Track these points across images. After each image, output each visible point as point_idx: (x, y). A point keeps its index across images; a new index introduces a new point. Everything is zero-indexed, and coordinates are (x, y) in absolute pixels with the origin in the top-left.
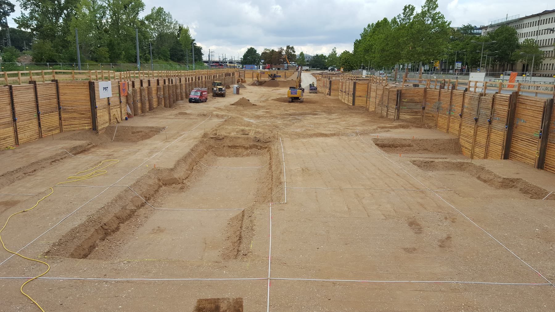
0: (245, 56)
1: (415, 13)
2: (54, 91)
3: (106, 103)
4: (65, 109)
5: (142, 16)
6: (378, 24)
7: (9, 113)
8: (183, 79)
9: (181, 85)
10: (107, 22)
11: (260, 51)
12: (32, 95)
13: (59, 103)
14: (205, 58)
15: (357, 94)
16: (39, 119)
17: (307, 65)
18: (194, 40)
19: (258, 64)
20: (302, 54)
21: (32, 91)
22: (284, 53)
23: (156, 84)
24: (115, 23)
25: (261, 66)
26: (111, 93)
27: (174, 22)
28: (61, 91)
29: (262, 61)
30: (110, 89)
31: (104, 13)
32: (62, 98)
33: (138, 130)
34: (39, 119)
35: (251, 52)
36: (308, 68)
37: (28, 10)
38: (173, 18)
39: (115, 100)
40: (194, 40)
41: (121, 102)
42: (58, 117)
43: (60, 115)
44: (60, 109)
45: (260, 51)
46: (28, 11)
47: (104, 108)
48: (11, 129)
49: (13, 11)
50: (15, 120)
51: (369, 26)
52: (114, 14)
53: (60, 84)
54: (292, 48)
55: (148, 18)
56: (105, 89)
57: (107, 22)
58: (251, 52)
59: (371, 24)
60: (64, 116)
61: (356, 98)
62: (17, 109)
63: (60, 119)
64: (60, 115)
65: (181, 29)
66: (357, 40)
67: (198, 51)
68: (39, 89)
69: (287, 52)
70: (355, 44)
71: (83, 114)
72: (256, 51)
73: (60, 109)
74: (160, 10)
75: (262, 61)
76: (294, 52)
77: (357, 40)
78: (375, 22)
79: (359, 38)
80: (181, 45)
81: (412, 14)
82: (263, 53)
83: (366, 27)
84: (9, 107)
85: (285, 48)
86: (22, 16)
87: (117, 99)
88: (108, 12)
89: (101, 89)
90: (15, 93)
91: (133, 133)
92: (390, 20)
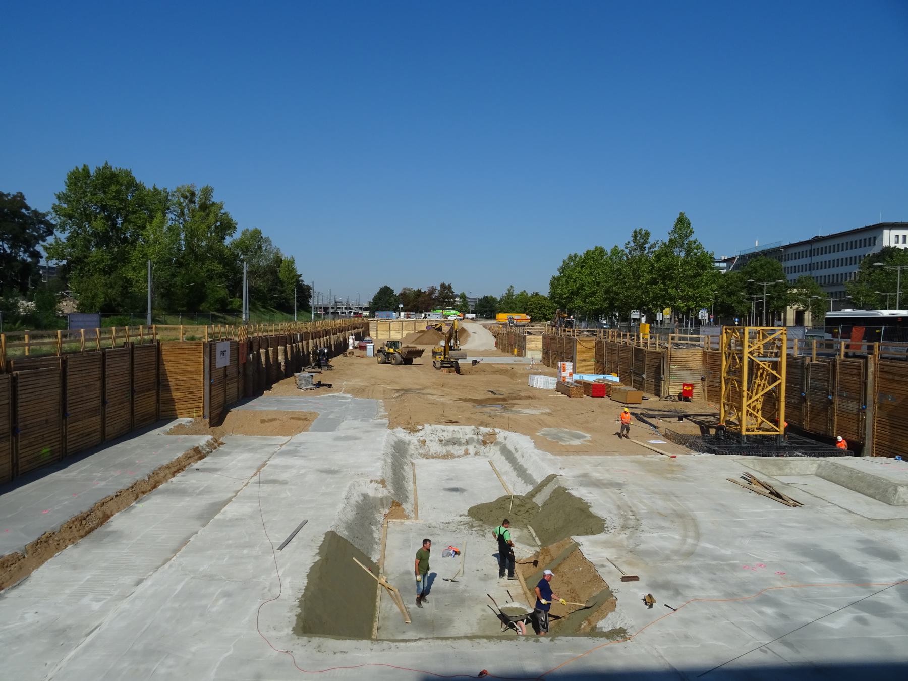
1: (651, 240)
3: (221, 374)
5: (228, 241)
11: (397, 292)
12: (127, 364)
16: (132, 403)
17: (473, 312)
18: (300, 276)
19: (396, 310)
20: (463, 296)
22: (437, 294)
25: (402, 314)
29: (401, 306)
30: (228, 353)
33: (270, 417)
34: (132, 403)
35: (385, 292)
36: (474, 316)
37: (67, 232)
38: (274, 244)
39: (232, 371)
40: (300, 276)
41: (239, 373)
42: (155, 398)
43: (158, 395)
44: (159, 383)
46: (67, 234)
47: (220, 383)
48: (98, 418)
49: (51, 233)
50: (104, 402)
51: (570, 257)
54: (450, 286)
56: (223, 352)
58: (385, 292)
59: (572, 255)
62: (108, 387)
63: (158, 401)
64: (158, 395)
65: (279, 261)
66: (554, 278)
67: (304, 292)
68: (137, 353)
70: (552, 284)
72: (392, 291)
73: (159, 383)
75: (401, 306)
77: (554, 278)
78: (581, 253)
79: (557, 274)
80: (282, 283)
81: (646, 242)
83: (566, 258)
84: (99, 384)
85: (439, 288)
87: (235, 370)
88: (182, 236)
90: (108, 361)
91: (263, 421)
92: (608, 250)
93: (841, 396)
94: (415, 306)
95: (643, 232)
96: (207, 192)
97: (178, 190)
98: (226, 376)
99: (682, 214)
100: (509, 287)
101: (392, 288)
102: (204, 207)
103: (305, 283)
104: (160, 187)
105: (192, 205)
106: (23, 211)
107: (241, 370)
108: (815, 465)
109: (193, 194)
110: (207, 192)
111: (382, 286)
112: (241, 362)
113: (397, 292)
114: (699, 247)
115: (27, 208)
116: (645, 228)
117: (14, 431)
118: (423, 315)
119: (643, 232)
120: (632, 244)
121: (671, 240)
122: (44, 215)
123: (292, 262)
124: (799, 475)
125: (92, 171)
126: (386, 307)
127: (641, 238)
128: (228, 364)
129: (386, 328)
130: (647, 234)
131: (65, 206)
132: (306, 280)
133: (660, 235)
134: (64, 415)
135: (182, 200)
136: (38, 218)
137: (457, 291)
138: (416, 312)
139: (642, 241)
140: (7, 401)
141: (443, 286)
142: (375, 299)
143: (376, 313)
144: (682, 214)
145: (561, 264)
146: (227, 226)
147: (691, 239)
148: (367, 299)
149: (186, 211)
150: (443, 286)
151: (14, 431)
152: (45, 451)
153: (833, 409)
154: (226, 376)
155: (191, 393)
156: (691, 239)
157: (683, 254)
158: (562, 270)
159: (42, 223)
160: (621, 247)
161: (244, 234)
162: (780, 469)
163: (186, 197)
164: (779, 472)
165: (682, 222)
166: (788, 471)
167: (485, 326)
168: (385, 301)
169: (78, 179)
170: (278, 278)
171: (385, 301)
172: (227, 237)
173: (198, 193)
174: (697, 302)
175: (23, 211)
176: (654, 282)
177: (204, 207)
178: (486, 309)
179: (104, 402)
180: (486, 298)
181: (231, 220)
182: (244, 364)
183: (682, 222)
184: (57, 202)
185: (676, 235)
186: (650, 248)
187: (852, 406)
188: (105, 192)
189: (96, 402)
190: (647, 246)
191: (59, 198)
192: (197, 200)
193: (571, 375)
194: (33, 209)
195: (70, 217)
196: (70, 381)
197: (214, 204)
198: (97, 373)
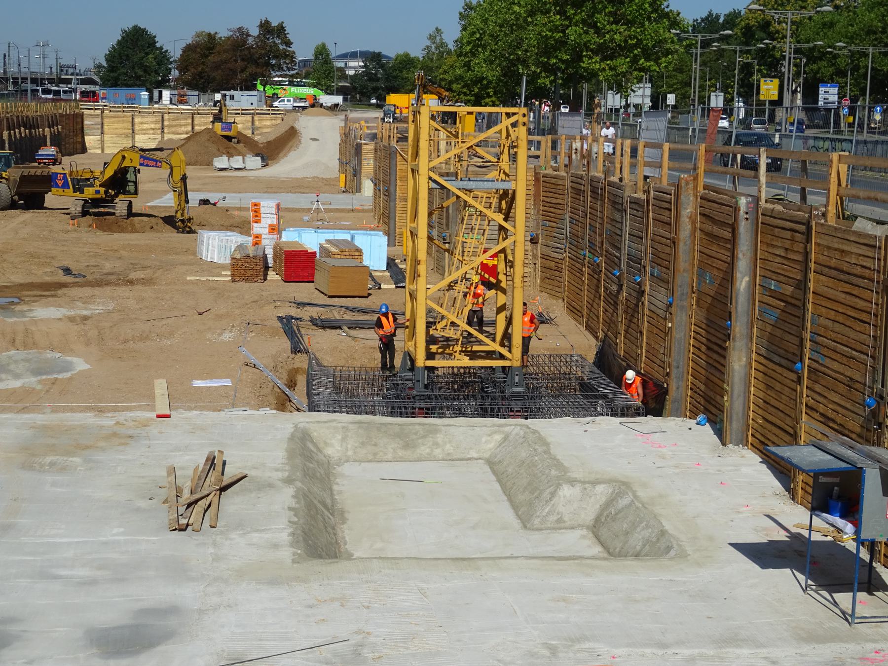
11: (173, 40)
17: (340, 91)
25: (166, 93)
36: (339, 99)
54: (280, 30)
76: (288, 43)
85: (255, 31)
93: (652, 275)
94: (200, 75)
101: (152, 30)
108: (498, 437)
111: (128, 25)
113: (173, 40)
118: (218, 96)
124: (449, 459)
126: (138, 78)
129: (123, 126)
138: (203, 90)
141: (265, 26)
142: (110, 58)
150: (265, 26)
153: (643, 303)
162: (407, 446)
164: (401, 453)
166: (424, 450)
168: (134, 63)
171: (134, 63)
174: (635, 60)
178: (376, 81)
187: (662, 297)
193: (272, 229)
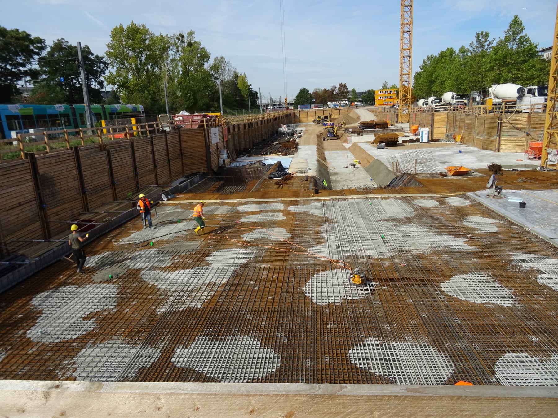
0: (298, 97)
1: (490, 39)
2: (177, 139)
3: (215, 148)
4: (186, 156)
5: (206, 66)
6: (442, 55)
7: (150, 161)
8: (259, 123)
9: (258, 128)
10: (178, 74)
11: (311, 91)
12: (164, 144)
13: (181, 150)
14: (259, 102)
15: (436, 125)
16: (169, 166)
17: (361, 102)
18: (250, 85)
20: (354, 91)
21: (164, 139)
23: (243, 128)
24: (186, 73)
26: (218, 138)
27: (234, 70)
28: (182, 138)
30: (217, 134)
31: (177, 65)
32: (183, 145)
34: (169, 166)
35: (304, 92)
37: (115, 68)
39: (221, 145)
40: (250, 85)
43: (182, 161)
44: (182, 155)
45: (389, 85)
49: (107, 68)
50: (155, 167)
51: (428, 58)
52: (185, 65)
53: (182, 133)
54: (345, 86)
55: (215, 68)
56: (215, 134)
57: (178, 74)
58: (304, 92)
59: (430, 56)
60: (185, 162)
61: (435, 130)
62: (156, 157)
63: (182, 164)
64: (182, 161)
65: (236, 76)
67: (254, 96)
69: (340, 89)
71: (200, 159)
72: (308, 91)
73: (182, 155)
74: (222, 58)
75: (314, 100)
78: (437, 54)
79: (419, 70)
82: (314, 93)
83: (425, 58)
84: (151, 155)
85: (338, 86)
86: (111, 74)
88: (180, 64)
89: (212, 135)
90: (155, 142)
95: (484, 33)
96: (191, 34)
97: (174, 35)
98: (218, 149)
99: (516, 17)
100: (384, 82)
101: (308, 89)
102: (190, 44)
103: (254, 90)
104: (164, 35)
105: (183, 44)
106: (90, 56)
107: (225, 145)
109: (183, 37)
110: (191, 34)
111: (302, 88)
112: (226, 139)
114: (528, 40)
115: (92, 54)
116: (485, 30)
117: (113, 183)
119: (484, 33)
120: (475, 43)
121: (506, 37)
122: (102, 58)
123: (245, 77)
125: (125, 28)
127: (482, 37)
128: (218, 141)
130: (487, 34)
131: (112, 51)
132: (255, 88)
133: (497, 35)
134: (136, 175)
135: (177, 41)
136: (99, 60)
137: (350, 89)
139: (483, 40)
140: (107, 167)
141: (341, 85)
142: (297, 97)
143: (299, 106)
144: (516, 17)
145: (421, 63)
146: (205, 56)
147: (523, 34)
148: (292, 97)
149: (180, 48)
150: (341, 85)
151: (113, 183)
152: (129, 194)
154: (218, 149)
155: (200, 159)
156: (523, 34)
157: (515, 47)
158: (422, 67)
159: (101, 62)
160: (467, 46)
161: (215, 60)
163: (179, 39)
165: (516, 24)
167: (369, 110)
168: (305, 98)
169: (117, 33)
170: (237, 88)
172: (205, 63)
173: (186, 36)
175: (90, 56)
176: (492, 69)
177: (190, 44)
179: (155, 167)
180: (369, 91)
181: (206, 52)
182: (227, 141)
183: (516, 24)
184: (108, 50)
185: (511, 32)
186: (489, 45)
188: (133, 40)
189: (151, 167)
190: (486, 44)
191: (108, 47)
192: (186, 40)
194: (95, 55)
195: (116, 57)
196: (137, 154)
197: (196, 42)
198: (149, 149)
